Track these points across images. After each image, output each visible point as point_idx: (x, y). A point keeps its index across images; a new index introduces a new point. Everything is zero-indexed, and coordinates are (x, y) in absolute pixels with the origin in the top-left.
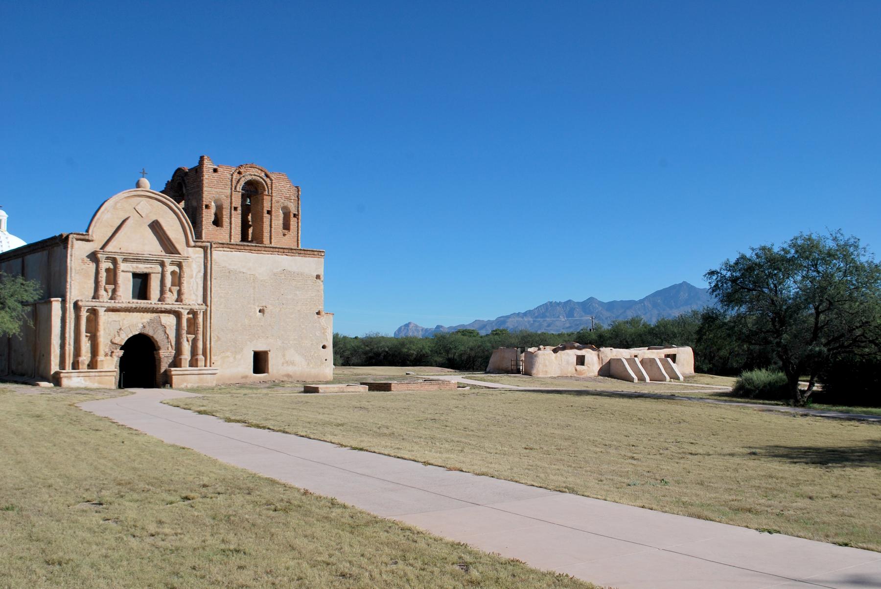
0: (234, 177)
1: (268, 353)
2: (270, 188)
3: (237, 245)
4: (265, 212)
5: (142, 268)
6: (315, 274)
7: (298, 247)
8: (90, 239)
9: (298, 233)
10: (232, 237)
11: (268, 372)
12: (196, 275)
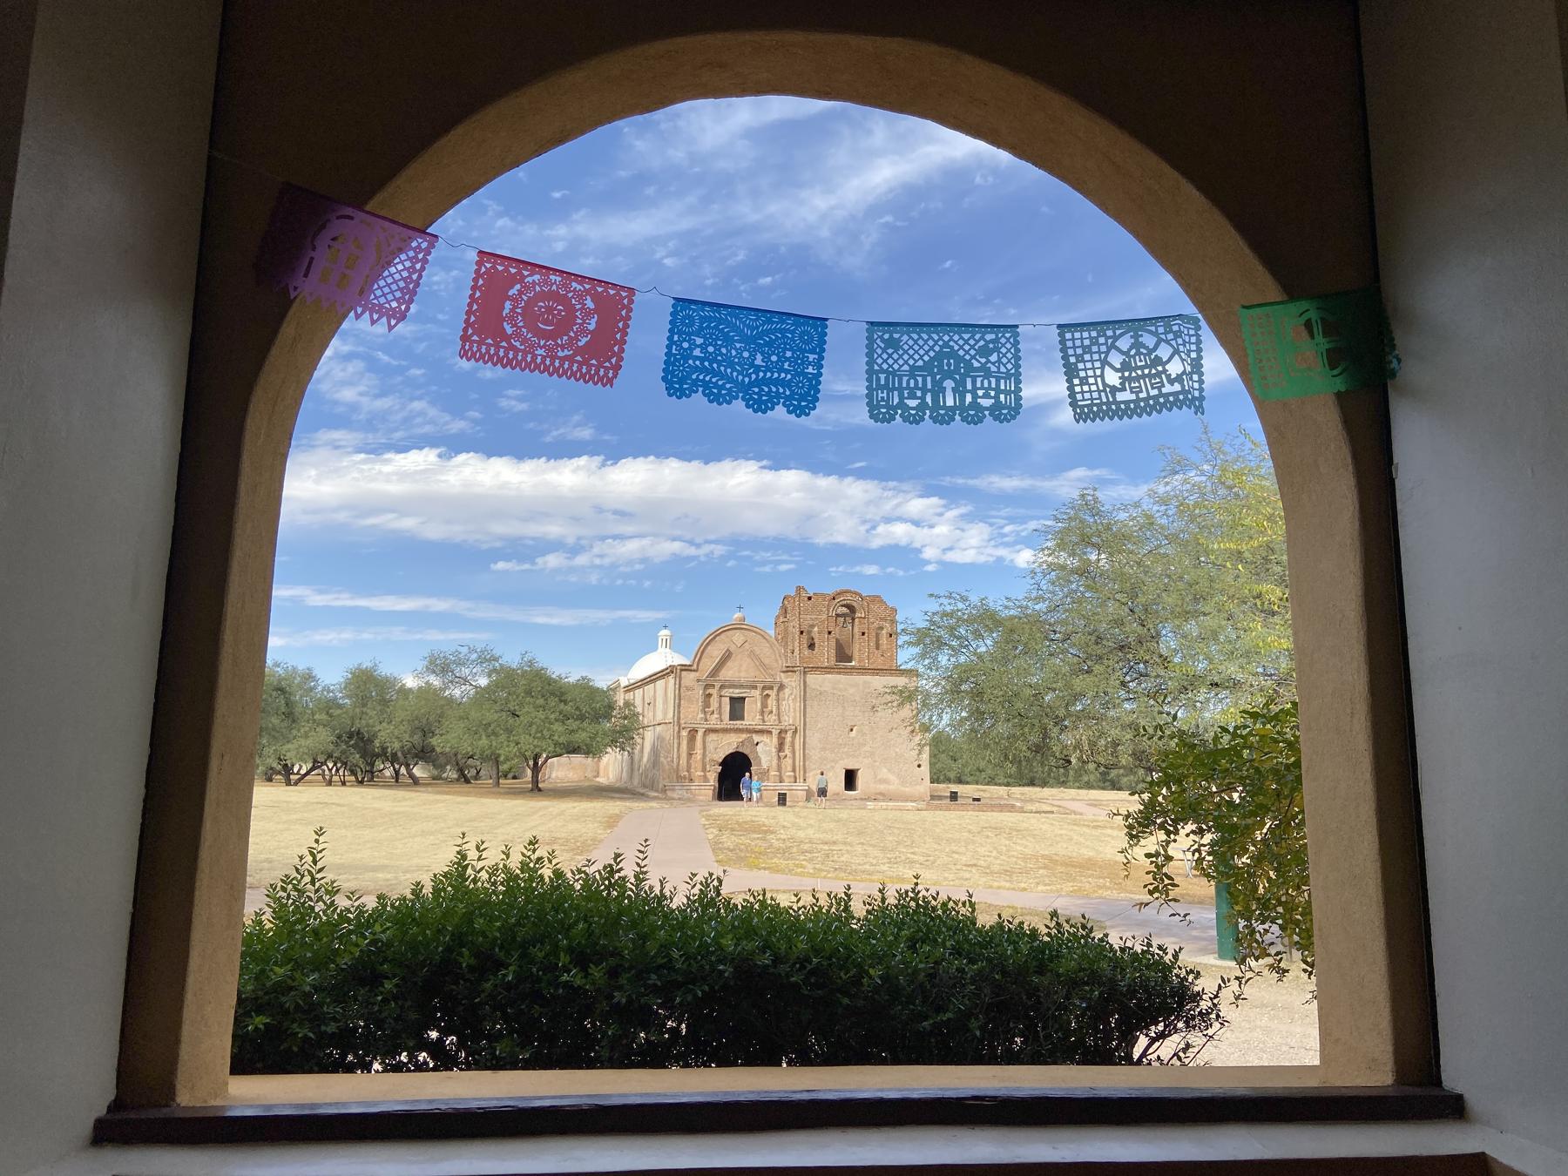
5: (736, 693)
8: (692, 668)
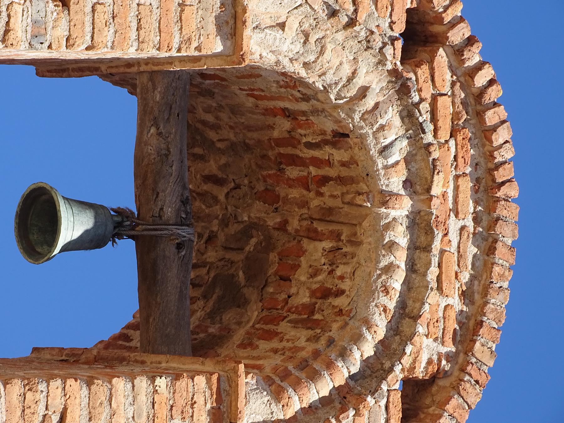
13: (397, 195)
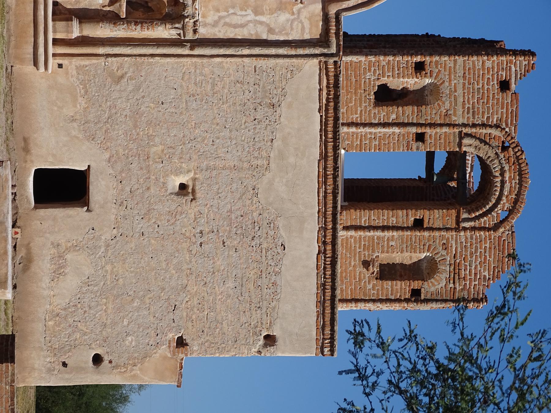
0: (495, 132)
1: (83, 207)
2: (477, 224)
3: (336, 168)
4: (419, 214)
6: (276, 332)
7: (340, 300)
9: (374, 301)
10: (353, 130)
11: (36, 208)
12: (261, 23)
13: (498, 177)
